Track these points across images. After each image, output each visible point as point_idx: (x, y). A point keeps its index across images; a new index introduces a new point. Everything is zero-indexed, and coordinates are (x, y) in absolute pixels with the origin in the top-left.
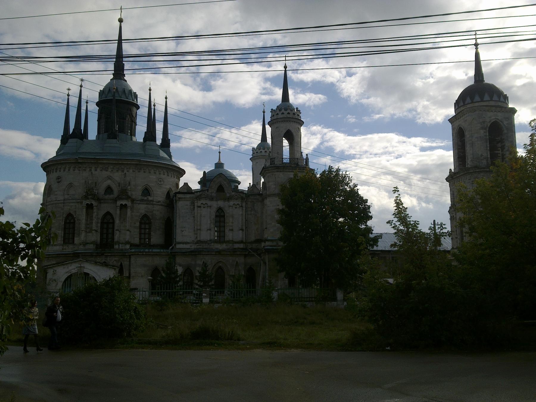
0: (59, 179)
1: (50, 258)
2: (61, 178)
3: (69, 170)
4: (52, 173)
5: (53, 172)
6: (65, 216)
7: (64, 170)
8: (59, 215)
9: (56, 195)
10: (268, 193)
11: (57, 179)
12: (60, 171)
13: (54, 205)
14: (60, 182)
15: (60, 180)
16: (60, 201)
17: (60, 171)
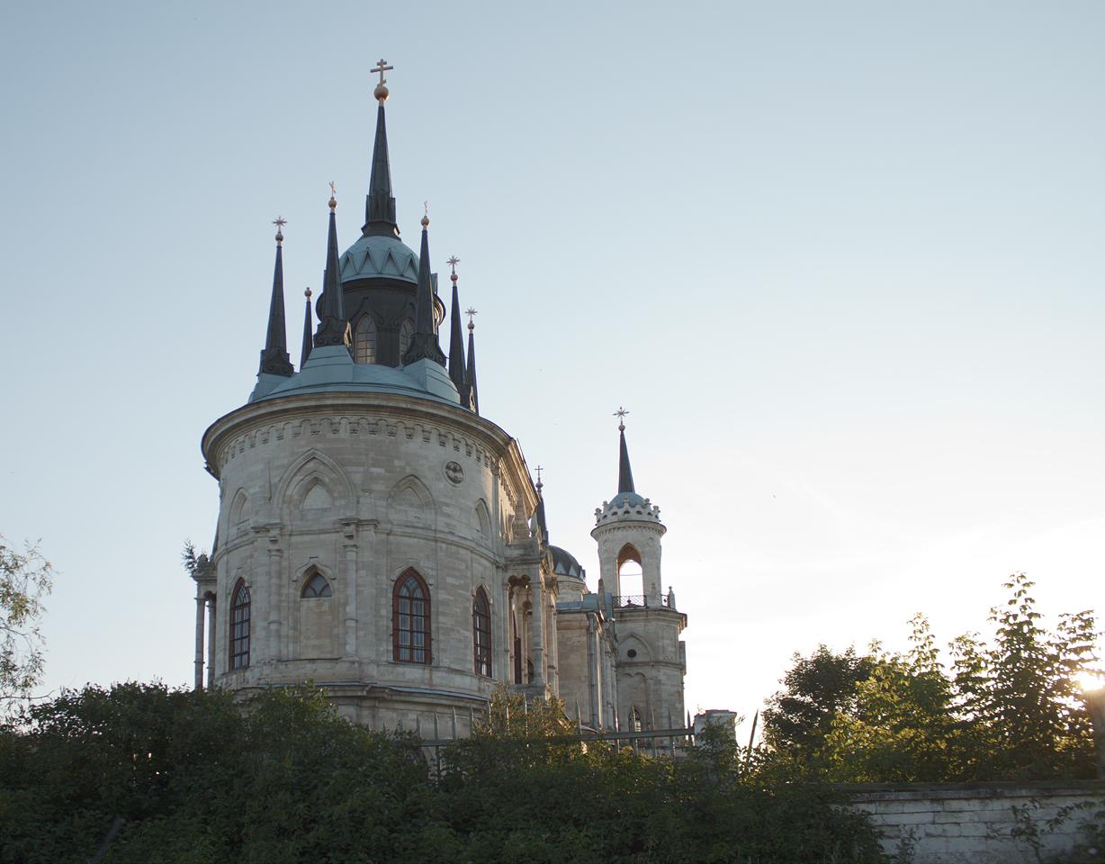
0: (455, 470)
1: (439, 709)
2: (461, 470)
3: (479, 459)
4: (418, 439)
5: (427, 440)
6: (474, 589)
7: (469, 453)
8: (462, 582)
9: (448, 516)
10: (661, 658)
11: (448, 467)
12: (457, 448)
13: (444, 545)
14: (460, 482)
15: (459, 475)
16: (468, 543)
17: (457, 448)
